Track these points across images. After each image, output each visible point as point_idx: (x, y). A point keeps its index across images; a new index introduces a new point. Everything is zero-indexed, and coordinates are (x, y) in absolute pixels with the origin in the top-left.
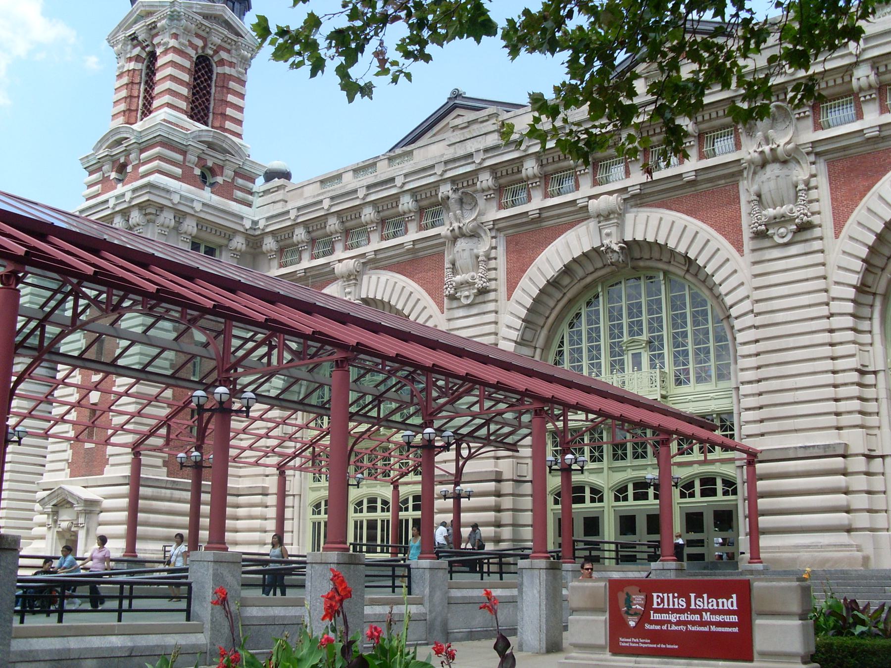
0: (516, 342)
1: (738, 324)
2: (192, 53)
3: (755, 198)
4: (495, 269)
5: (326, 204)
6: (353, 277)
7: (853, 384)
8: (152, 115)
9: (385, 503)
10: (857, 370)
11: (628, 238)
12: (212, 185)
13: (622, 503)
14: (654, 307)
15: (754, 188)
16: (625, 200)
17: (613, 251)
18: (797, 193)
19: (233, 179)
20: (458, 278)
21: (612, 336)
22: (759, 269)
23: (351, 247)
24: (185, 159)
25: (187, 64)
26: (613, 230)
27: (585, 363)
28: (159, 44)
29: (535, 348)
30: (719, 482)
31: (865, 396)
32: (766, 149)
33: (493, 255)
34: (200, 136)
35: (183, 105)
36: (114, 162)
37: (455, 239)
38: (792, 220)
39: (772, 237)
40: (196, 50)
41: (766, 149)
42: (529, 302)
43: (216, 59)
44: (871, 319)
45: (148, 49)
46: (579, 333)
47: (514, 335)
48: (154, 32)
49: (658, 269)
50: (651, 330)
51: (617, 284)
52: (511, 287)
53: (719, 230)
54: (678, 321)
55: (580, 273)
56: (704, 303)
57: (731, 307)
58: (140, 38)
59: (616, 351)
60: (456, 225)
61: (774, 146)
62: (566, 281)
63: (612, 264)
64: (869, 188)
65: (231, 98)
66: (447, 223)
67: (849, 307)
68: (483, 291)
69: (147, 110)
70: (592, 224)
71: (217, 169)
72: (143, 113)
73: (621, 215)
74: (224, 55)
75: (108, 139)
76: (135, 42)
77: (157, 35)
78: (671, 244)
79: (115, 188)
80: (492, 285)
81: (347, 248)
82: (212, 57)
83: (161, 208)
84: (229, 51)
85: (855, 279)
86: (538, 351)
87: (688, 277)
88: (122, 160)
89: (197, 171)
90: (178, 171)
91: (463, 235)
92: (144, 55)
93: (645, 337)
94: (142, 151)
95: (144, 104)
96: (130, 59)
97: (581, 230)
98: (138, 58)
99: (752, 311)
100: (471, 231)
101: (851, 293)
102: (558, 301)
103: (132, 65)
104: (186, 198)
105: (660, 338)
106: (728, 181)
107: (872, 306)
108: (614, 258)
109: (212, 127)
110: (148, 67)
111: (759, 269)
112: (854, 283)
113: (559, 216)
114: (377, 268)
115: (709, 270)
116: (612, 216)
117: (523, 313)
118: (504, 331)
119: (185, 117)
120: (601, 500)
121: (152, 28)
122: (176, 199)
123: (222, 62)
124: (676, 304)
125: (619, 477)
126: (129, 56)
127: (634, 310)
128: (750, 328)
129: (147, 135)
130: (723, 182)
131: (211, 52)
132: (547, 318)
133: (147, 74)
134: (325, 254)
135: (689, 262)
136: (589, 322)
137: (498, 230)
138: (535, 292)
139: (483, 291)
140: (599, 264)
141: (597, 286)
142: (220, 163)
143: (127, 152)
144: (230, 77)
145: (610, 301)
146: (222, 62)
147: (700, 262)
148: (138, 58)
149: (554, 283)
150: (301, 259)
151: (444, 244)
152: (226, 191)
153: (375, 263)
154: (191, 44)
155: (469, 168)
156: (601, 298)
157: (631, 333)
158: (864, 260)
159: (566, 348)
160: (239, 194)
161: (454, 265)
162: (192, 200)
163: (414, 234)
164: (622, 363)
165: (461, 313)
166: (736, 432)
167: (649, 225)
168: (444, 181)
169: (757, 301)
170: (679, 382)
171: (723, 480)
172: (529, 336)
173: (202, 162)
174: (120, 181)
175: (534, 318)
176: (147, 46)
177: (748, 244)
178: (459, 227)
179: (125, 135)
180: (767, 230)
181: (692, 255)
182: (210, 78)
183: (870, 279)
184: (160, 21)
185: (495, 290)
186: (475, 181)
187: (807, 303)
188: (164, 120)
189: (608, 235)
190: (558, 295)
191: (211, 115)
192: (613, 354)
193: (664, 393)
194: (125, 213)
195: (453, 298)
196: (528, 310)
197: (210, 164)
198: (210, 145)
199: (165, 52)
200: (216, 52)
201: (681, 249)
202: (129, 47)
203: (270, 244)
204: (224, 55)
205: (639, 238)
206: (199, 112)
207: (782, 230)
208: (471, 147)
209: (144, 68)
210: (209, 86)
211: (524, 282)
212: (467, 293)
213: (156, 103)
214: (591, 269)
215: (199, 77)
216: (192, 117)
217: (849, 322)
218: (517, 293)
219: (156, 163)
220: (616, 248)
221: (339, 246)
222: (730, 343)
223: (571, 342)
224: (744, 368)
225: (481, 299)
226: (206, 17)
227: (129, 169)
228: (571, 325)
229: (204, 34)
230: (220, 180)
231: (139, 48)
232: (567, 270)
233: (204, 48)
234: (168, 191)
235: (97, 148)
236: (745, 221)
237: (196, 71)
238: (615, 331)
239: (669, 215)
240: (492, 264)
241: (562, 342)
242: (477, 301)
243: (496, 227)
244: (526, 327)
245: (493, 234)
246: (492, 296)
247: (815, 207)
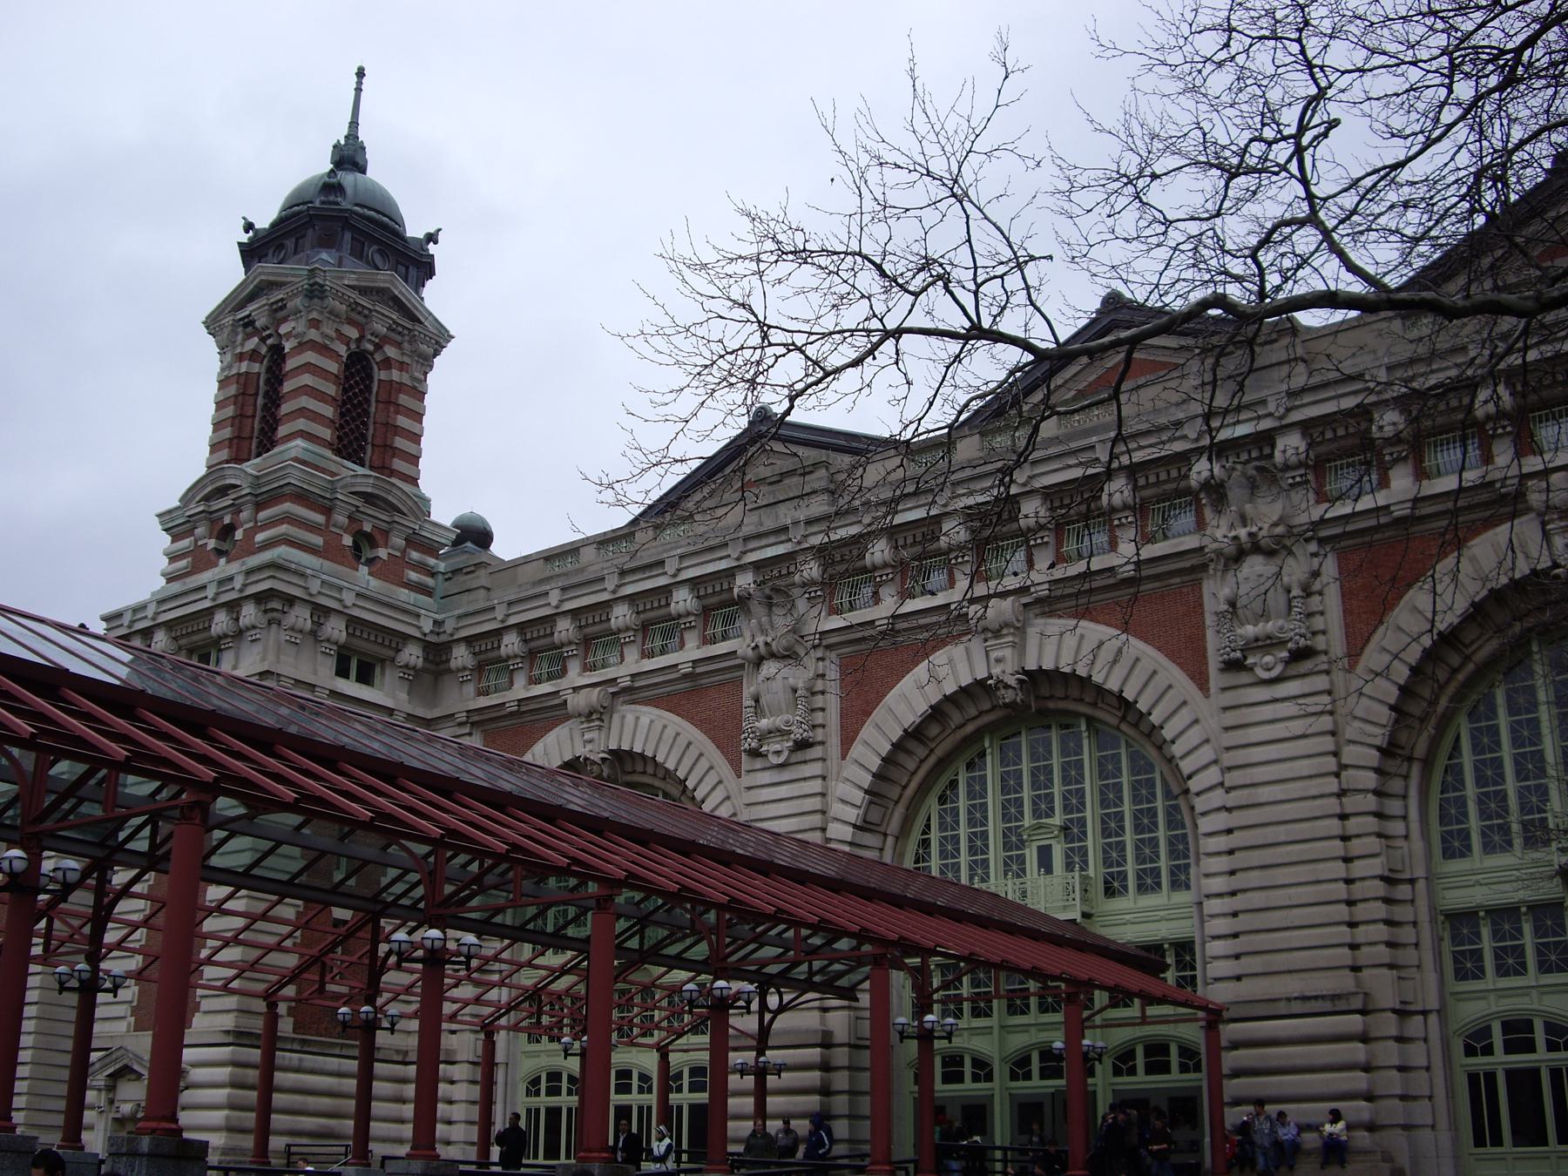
0: (854, 826)
1: (1200, 804)
2: (342, 350)
3: (1225, 607)
4: (823, 710)
5: (554, 597)
6: (597, 716)
7: (1376, 899)
8: (276, 450)
9: (644, 1078)
10: (1382, 878)
11: (1031, 665)
12: (370, 562)
13: (1021, 1083)
14: (1072, 773)
15: (1226, 592)
16: (1025, 605)
17: (1007, 686)
18: (1290, 601)
19: (404, 552)
20: (764, 723)
21: (1006, 817)
22: (1231, 718)
23: (593, 668)
24: (328, 520)
25: (333, 367)
27: (964, 859)
28: (289, 335)
29: (885, 835)
30: (1174, 1050)
31: (1396, 918)
32: (1242, 533)
33: (819, 685)
34: (353, 485)
35: (326, 433)
36: (213, 522)
37: (758, 662)
38: (1282, 643)
39: (1252, 669)
40: (348, 345)
41: (1242, 533)
42: (875, 763)
43: (378, 357)
44: (1405, 797)
45: (269, 342)
46: (955, 812)
47: (852, 815)
48: (281, 314)
49: (1078, 715)
50: (1067, 808)
51: (1014, 735)
52: (847, 741)
53: (1172, 656)
54: (1110, 796)
55: (956, 717)
56: (1150, 768)
57: (1190, 777)
58: (258, 324)
59: (1014, 841)
60: (760, 640)
61: (1254, 529)
62: (934, 730)
63: (1006, 705)
65: (402, 421)
66: (747, 634)
67: (1370, 780)
68: (803, 745)
69: (267, 441)
70: (976, 645)
71: (378, 537)
72: (260, 443)
73: (1021, 631)
74: (391, 351)
75: (205, 486)
76: (250, 329)
77: (285, 320)
78: (1097, 678)
79: (216, 565)
80: (819, 735)
81: (588, 668)
82: (372, 354)
83: (291, 600)
84: (399, 345)
85: (1379, 736)
86: (890, 840)
87: (1124, 727)
88: (227, 520)
89: (348, 540)
90: (318, 540)
91: (773, 655)
92: (264, 350)
93: (1057, 819)
94: (259, 507)
95: (262, 429)
96: (240, 357)
97: (956, 651)
98: (254, 355)
99: (1222, 784)
100: (786, 649)
101: (1373, 757)
102: (922, 761)
103: (244, 367)
104: (331, 586)
105: (1082, 822)
106: (1185, 578)
107: (1406, 777)
108: (1009, 696)
109: (371, 468)
110: (269, 370)
111: (1231, 718)
112: (1378, 742)
114: (633, 702)
115: (1155, 718)
116: (1005, 631)
117: (866, 780)
118: (837, 809)
119: (329, 453)
120: (989, 1077)
121: (278, 312)
122: (315, 586)
123: (387, 363)
124: (1107, 769)
125: (1018, 1041)
126: (238, 350)
127: (1041, 777)
128: (1218, 809)
129: (270, 482)
130: (1177, 580)
131: (370, 347)
132: (905, 787)
133: (268, 382)
134: (550, 677)
135: (1125, 706)
136: (971, 795)
137: (828, 647)
138: (885, 748)
139: (803, 745)
140: (986, 706)
141: (982, 739)
142: (384, 526)
143: (236, 509)
144: (401, 387)
145: (1004, 762)
146: (387, 363)
147: (1142, 706)
148: (254, 355)
149: (915, 734)
150: (512, 683)
151: (741, 666)
152: (391, 572)
153: (632, 693)
154: (341, 336)
155: (781, 550)
156: (989, 758)
157: (1037, 813)
158: (1392, 708)
159: (934, 835)
160: (413, 576)
161: (757, 701)
162: (340, 589)
163: (691, 651)
164: (1021, 860)
165: (767, 777)
166: (1198, 973)
167: (1061, 644)
168: (742, 568)
169: (1230, 769)
170: (1110, 892)
171: (1180, 1047)
172: (875, 816)
173: (355, 527)
174: (220, 553)
175: (884, 788)
176: (269, 336)
177: (1216, 679)
179: (233, 481)
180: (1245, 658)
181: (1129, 695)
182: (369, 389)
183: (1403, 737)
184: (291, 298)
185: (822, 743)
186: (792, 569)
187: (1306, 773)
188: (296, 459)
189: (998, 661)
190: (921, 752)
191: (369, 448)
192: (1007, 846)
193: (1086, 909)
194: (233, 607)
195: (755, 753)
196: (874, 775)
197: (367, 528)
198: (368, 498)
199: (302, 347)
200: (378, 347)
201: (1113, 685)
202: (240, 337)
203: (461, 656)
204: (391, 351)
205: (1048, 665)
206: (350, 442)
207: (1268, 659)
208: (786, 515)
209: (263, 370)
210: (368, 401)
211: (867, 731)
212: (778, 747)
213: (283, 431)
214: (973, 712)
215: (351, 387)
216: (338, 452)
217: (1371, 802)
218: (857, 750)
219: (283, 528)
220: (1012, 681)
221: (574, 668)
222: (1189, 830)
223: (943, 826)
224: (1210, 873)
225: (799, 756)
226: (363, 291)
227: (239, 535)
228: (942, 800)
229: (361, 319)
230: (382, 553)
231: (256, 339)
232: (936, 713)
233: (359, 340)
234: (303, 575)
235: (186, 499)
236: (1212, 642)
237: (346, 377)
238: (1011, 810)
239: (1093, 631)
240: (819, 701)
241: (928, 826)
242: (793, 760)
243: (825, 643)
244: (871, 802)
245: (819, 653)
246: (817, 752)
247: (1318, 623)
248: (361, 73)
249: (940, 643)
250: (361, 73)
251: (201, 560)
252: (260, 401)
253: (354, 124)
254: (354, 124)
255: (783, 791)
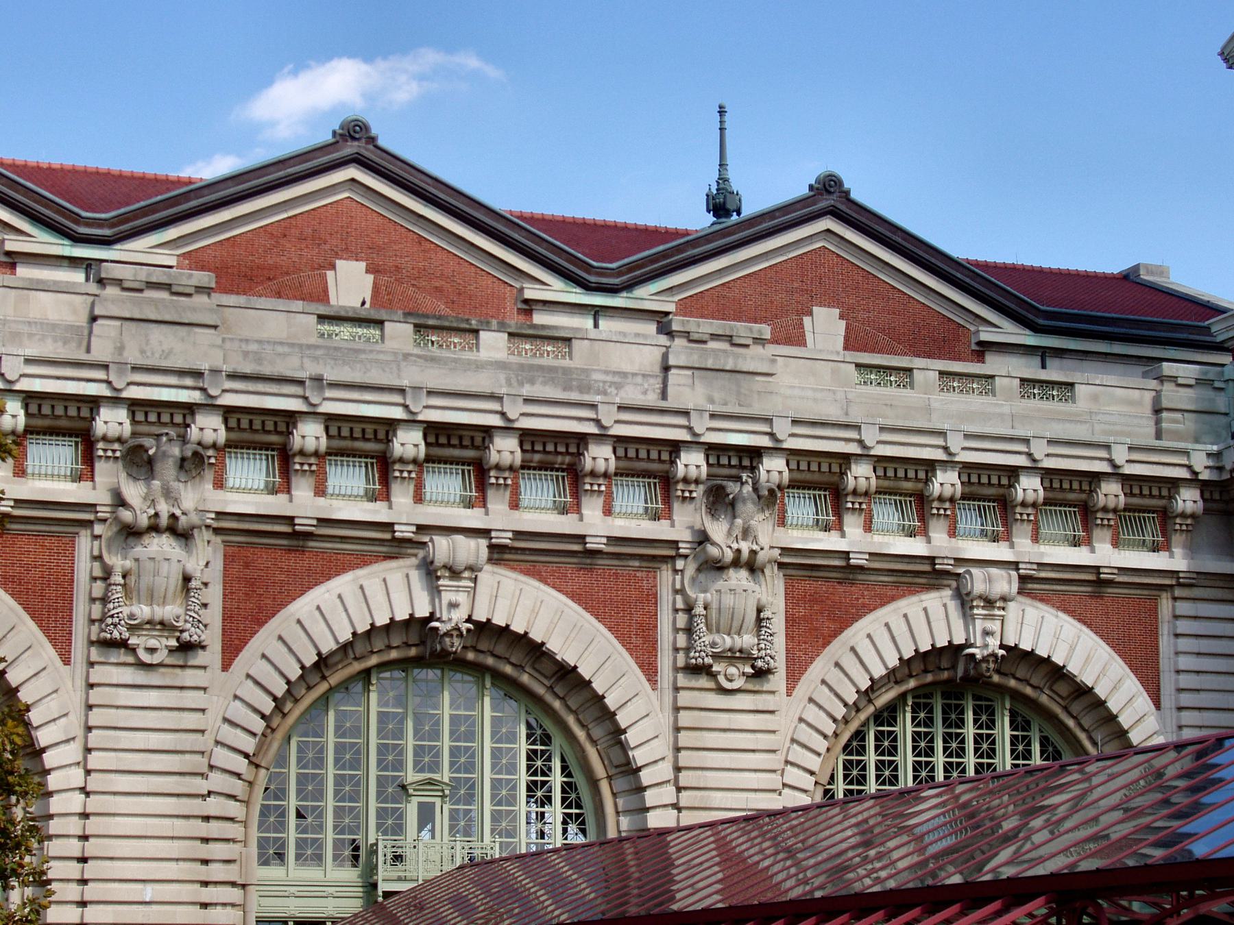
11: (481, 616)
20: (143, 611)
26: (462, 598)
32: (745, 547)
41: (745, 547)
60: (164, 508)
64: (836, 634)
106: (645, 564)
113: (343, 539)
130: (637, 563)
178: (173, 516)
212: (153, 643)
249: (363, 561)
255: (152, 698)
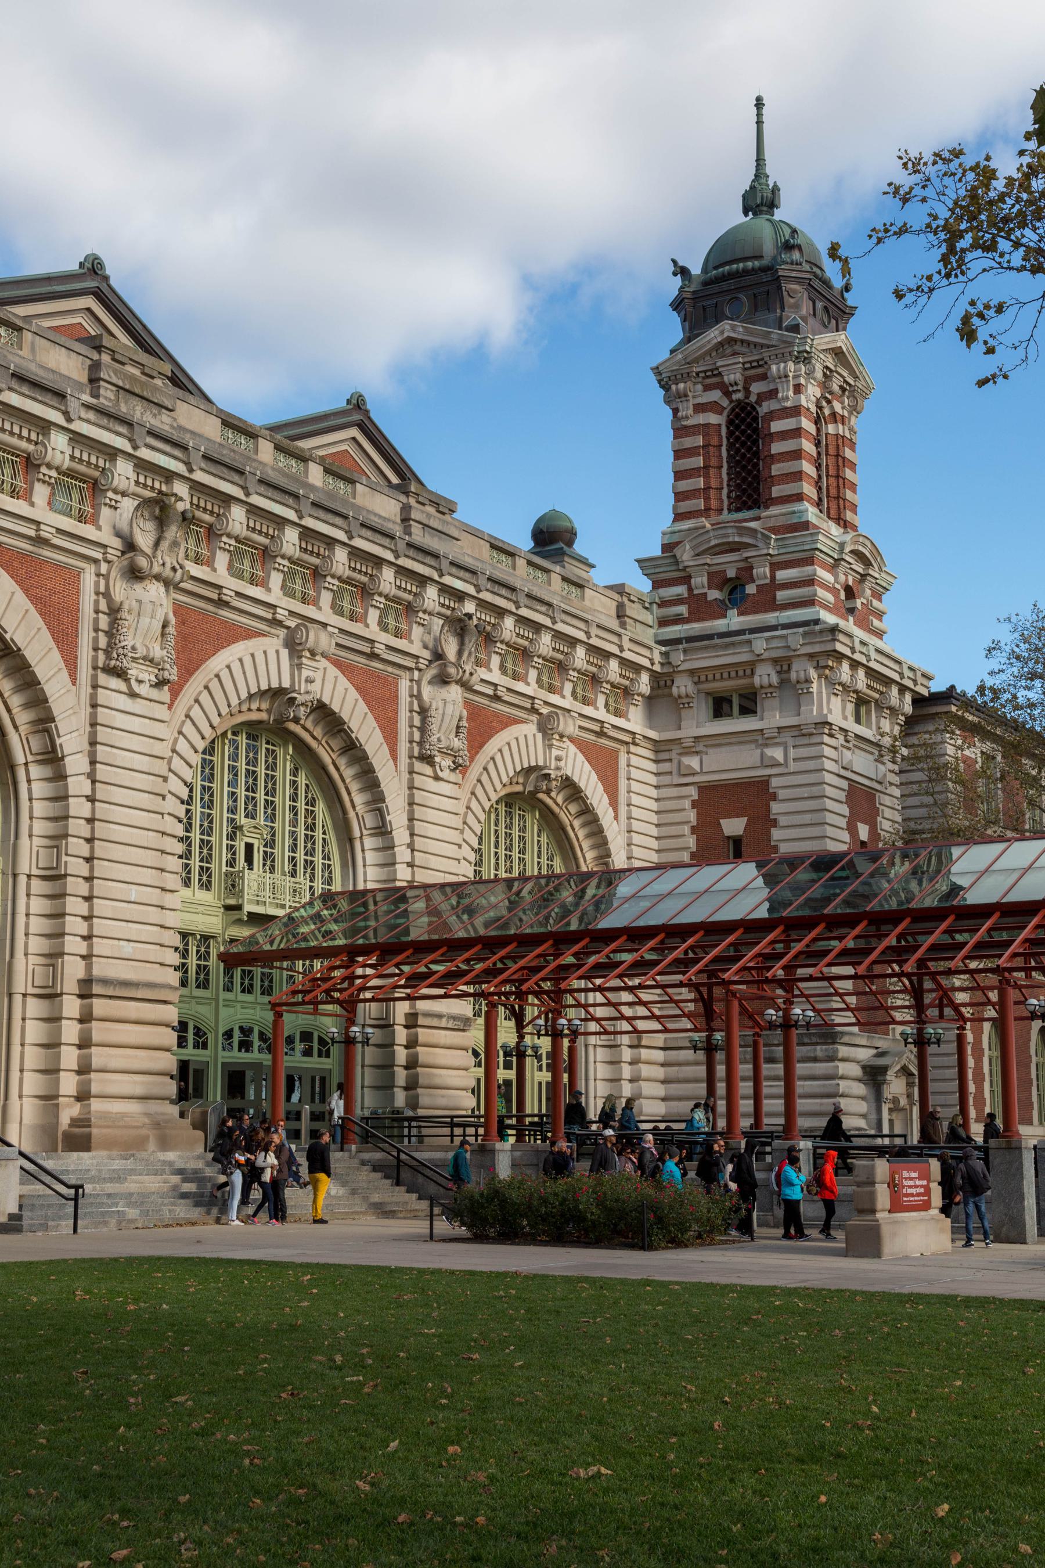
88: (731, 573)
94: (775, 566)
96: (700, 408)
110: (730, 422)
126: (700, 400)
204: (837, 407)
227: (751, 589)
248: (759, 103)
250: (759, 103)
251: (700, 608)
252: (724, 453)
253: (760, 161)
254: (760, 161)
